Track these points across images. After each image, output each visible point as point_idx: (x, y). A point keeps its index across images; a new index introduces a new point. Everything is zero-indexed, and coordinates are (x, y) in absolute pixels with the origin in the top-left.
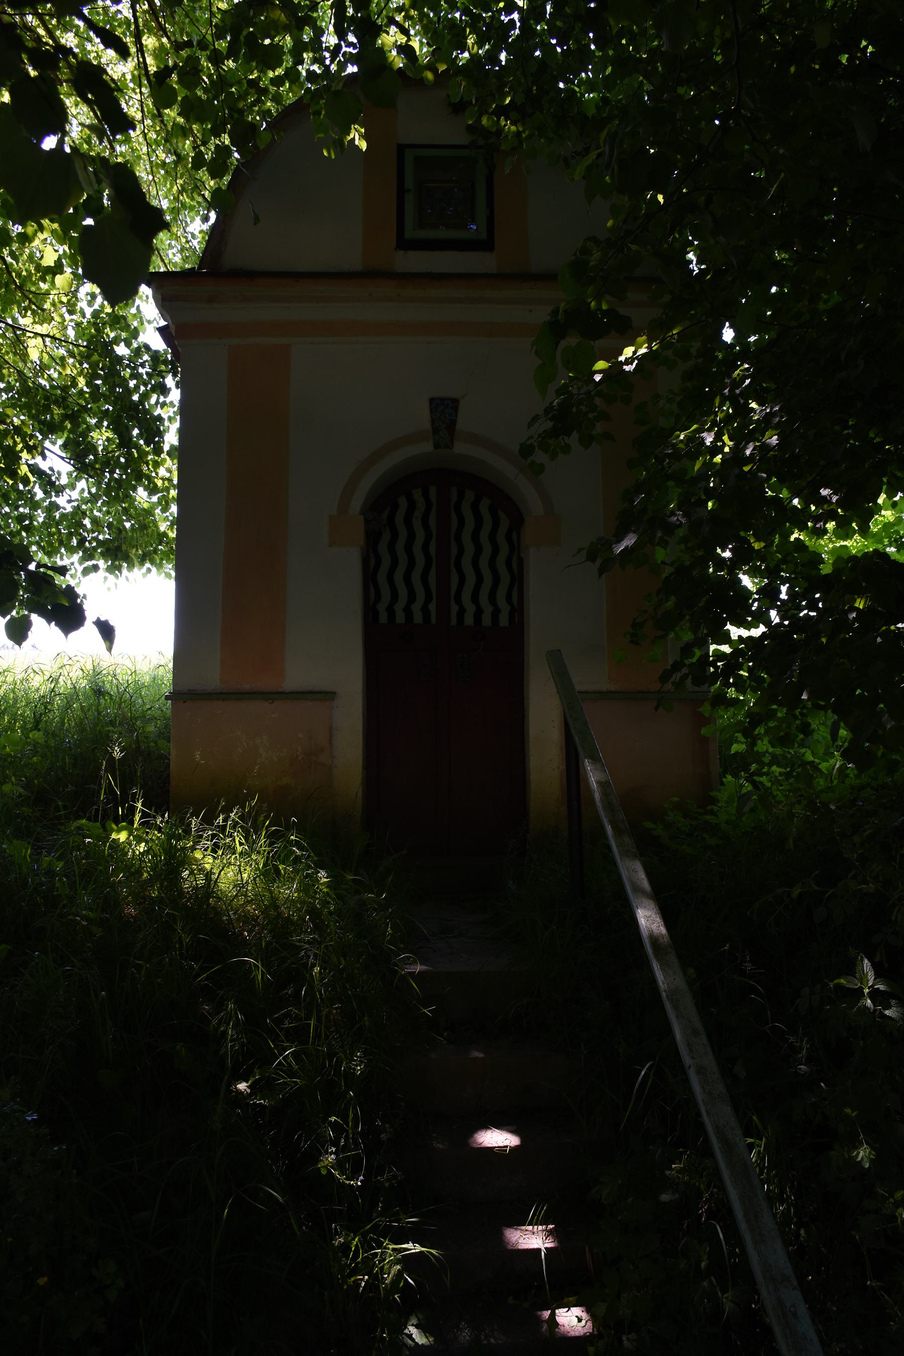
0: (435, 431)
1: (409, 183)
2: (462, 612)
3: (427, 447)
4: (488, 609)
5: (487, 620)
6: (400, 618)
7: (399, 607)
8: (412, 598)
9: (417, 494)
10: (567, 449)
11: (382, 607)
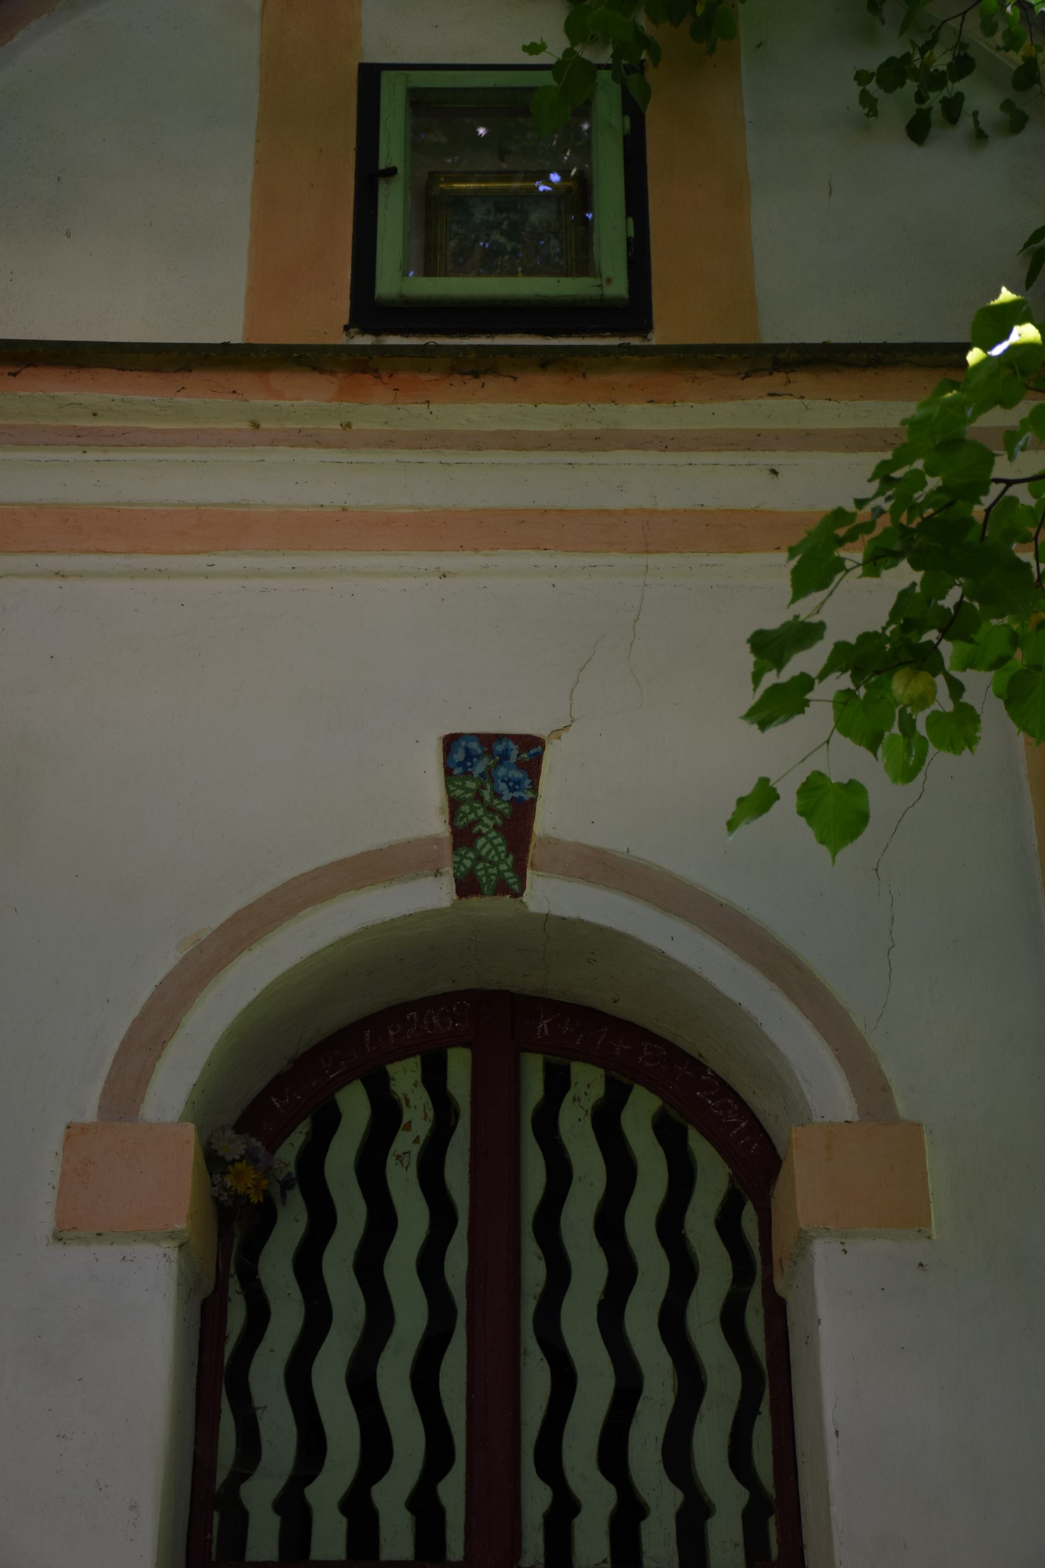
0: (463, 837)
1: (392, 150)
3: (436, 893)
4: (663, 1500)
7: (327, 1492)
9: (406, 1078)
10: (960, 727)
11: (260, 1493)
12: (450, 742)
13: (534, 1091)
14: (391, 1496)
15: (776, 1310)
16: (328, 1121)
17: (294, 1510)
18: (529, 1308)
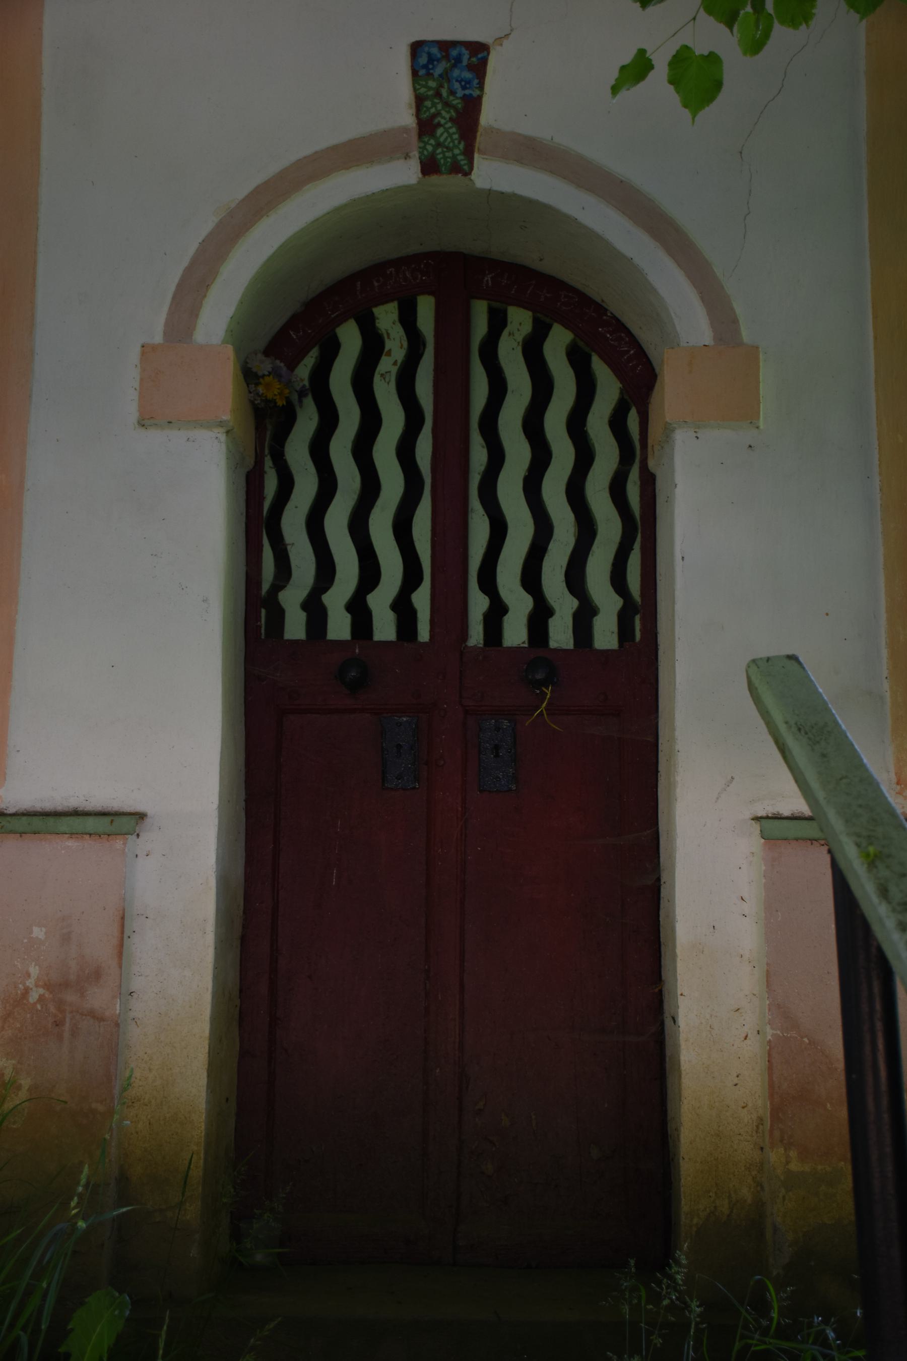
0: (426, 127)
2: (497, 611)
4: (564, 605)
5: (561, 634)
6: (339, 627)
7: (336, 600)
8: (370, 574)
9: (387, 317)
11: (291, 601)
12: (416, 48)
13: (480, 327)
14: (380, 602)
15: (649, 481)
17: (315, 609)
18: (475, 480)
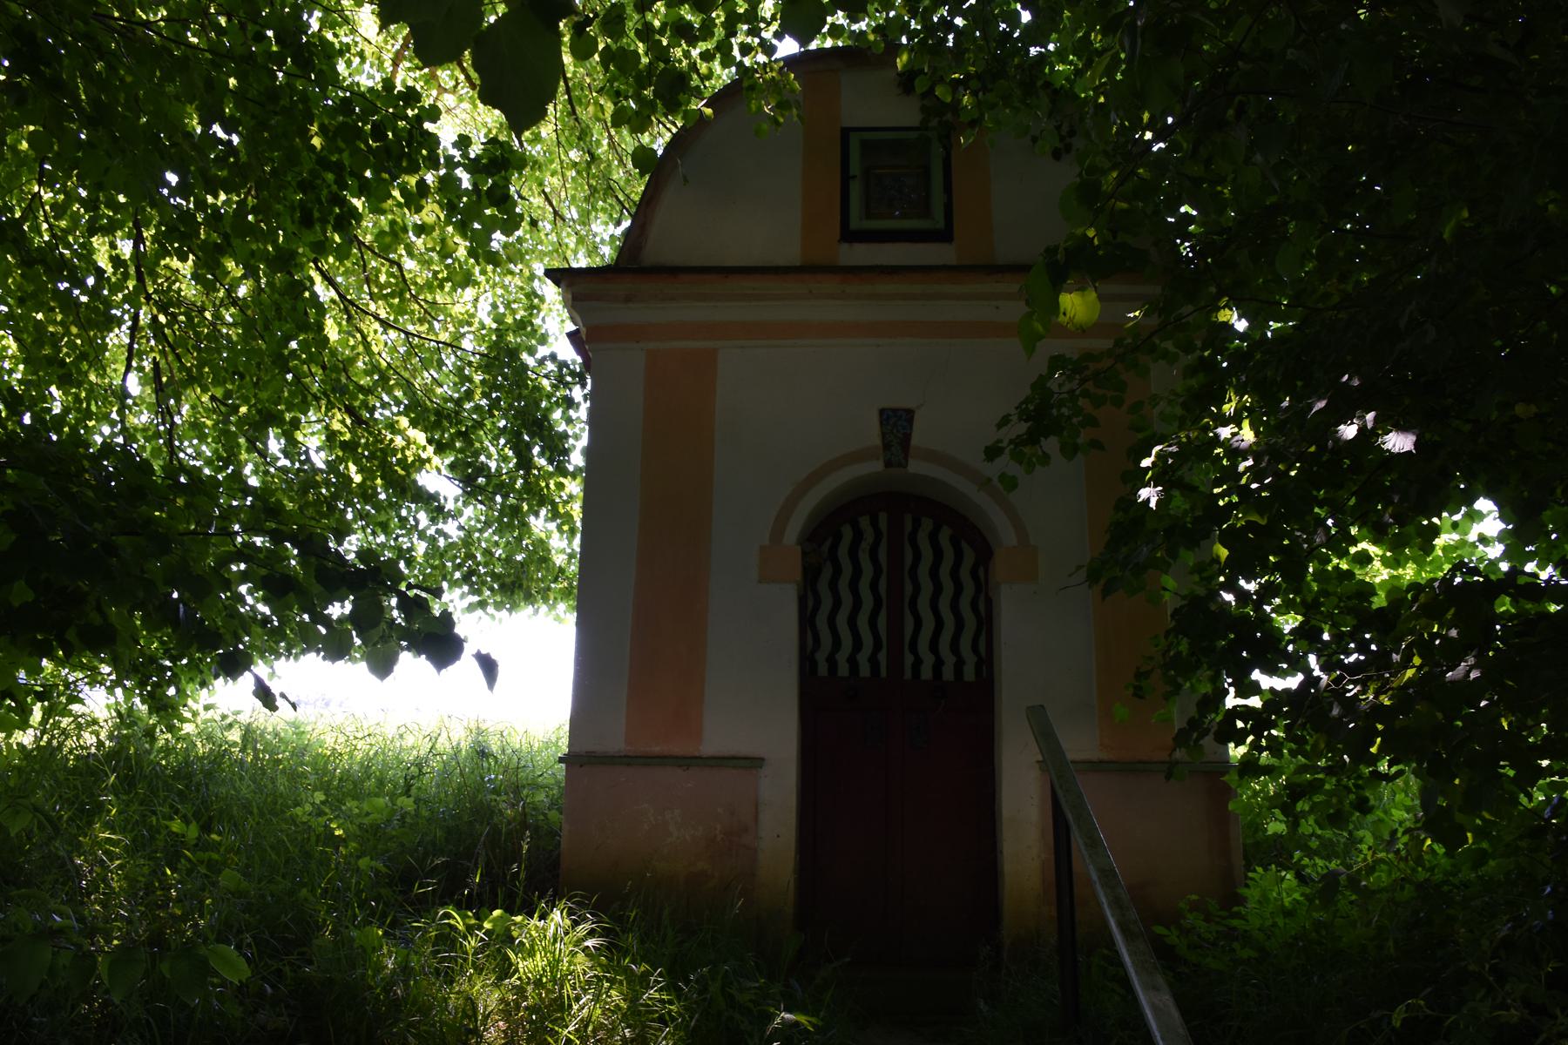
0: (887, 446)
1: (855, 167)
2: (918, 662)
3: (877, 466)
5: (948, 674)
6: (843, 670)
7: (842, 657)
8: (858, 645)
9: (864, 522)
10: (1045, 459)
11: (821, 657)
12: (882, 412)
13: (908, 527)
14: (863, 658)
15: (989, 602)
16: (838, 537)
17: (832, 662)
18: (907, 600)
